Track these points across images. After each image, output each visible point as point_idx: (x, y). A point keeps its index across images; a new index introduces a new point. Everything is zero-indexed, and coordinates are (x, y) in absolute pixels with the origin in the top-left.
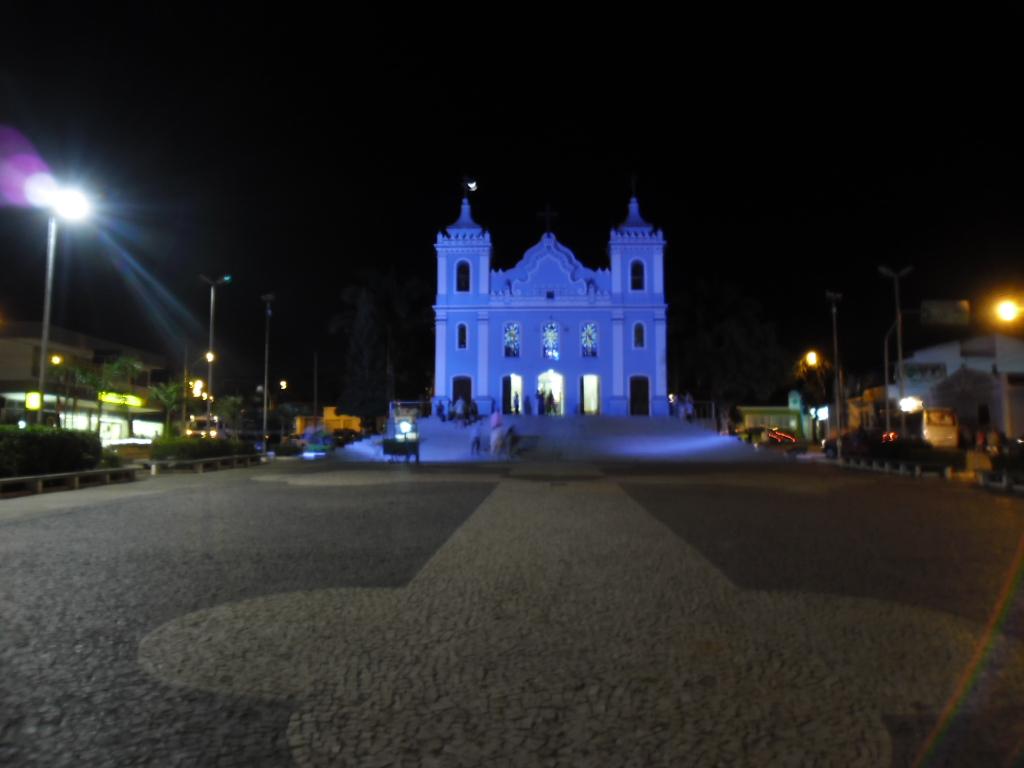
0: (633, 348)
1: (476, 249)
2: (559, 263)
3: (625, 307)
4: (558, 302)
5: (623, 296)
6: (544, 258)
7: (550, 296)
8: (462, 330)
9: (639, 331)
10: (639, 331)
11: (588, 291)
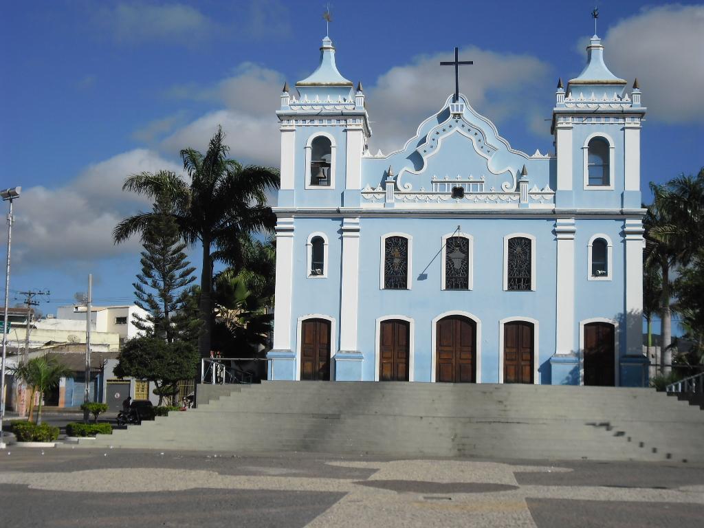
0: (590, 278)
6: (453, 131)
7: (458, 193)
9: (600, 248)
10: (600, 248)
11: (518, 187)
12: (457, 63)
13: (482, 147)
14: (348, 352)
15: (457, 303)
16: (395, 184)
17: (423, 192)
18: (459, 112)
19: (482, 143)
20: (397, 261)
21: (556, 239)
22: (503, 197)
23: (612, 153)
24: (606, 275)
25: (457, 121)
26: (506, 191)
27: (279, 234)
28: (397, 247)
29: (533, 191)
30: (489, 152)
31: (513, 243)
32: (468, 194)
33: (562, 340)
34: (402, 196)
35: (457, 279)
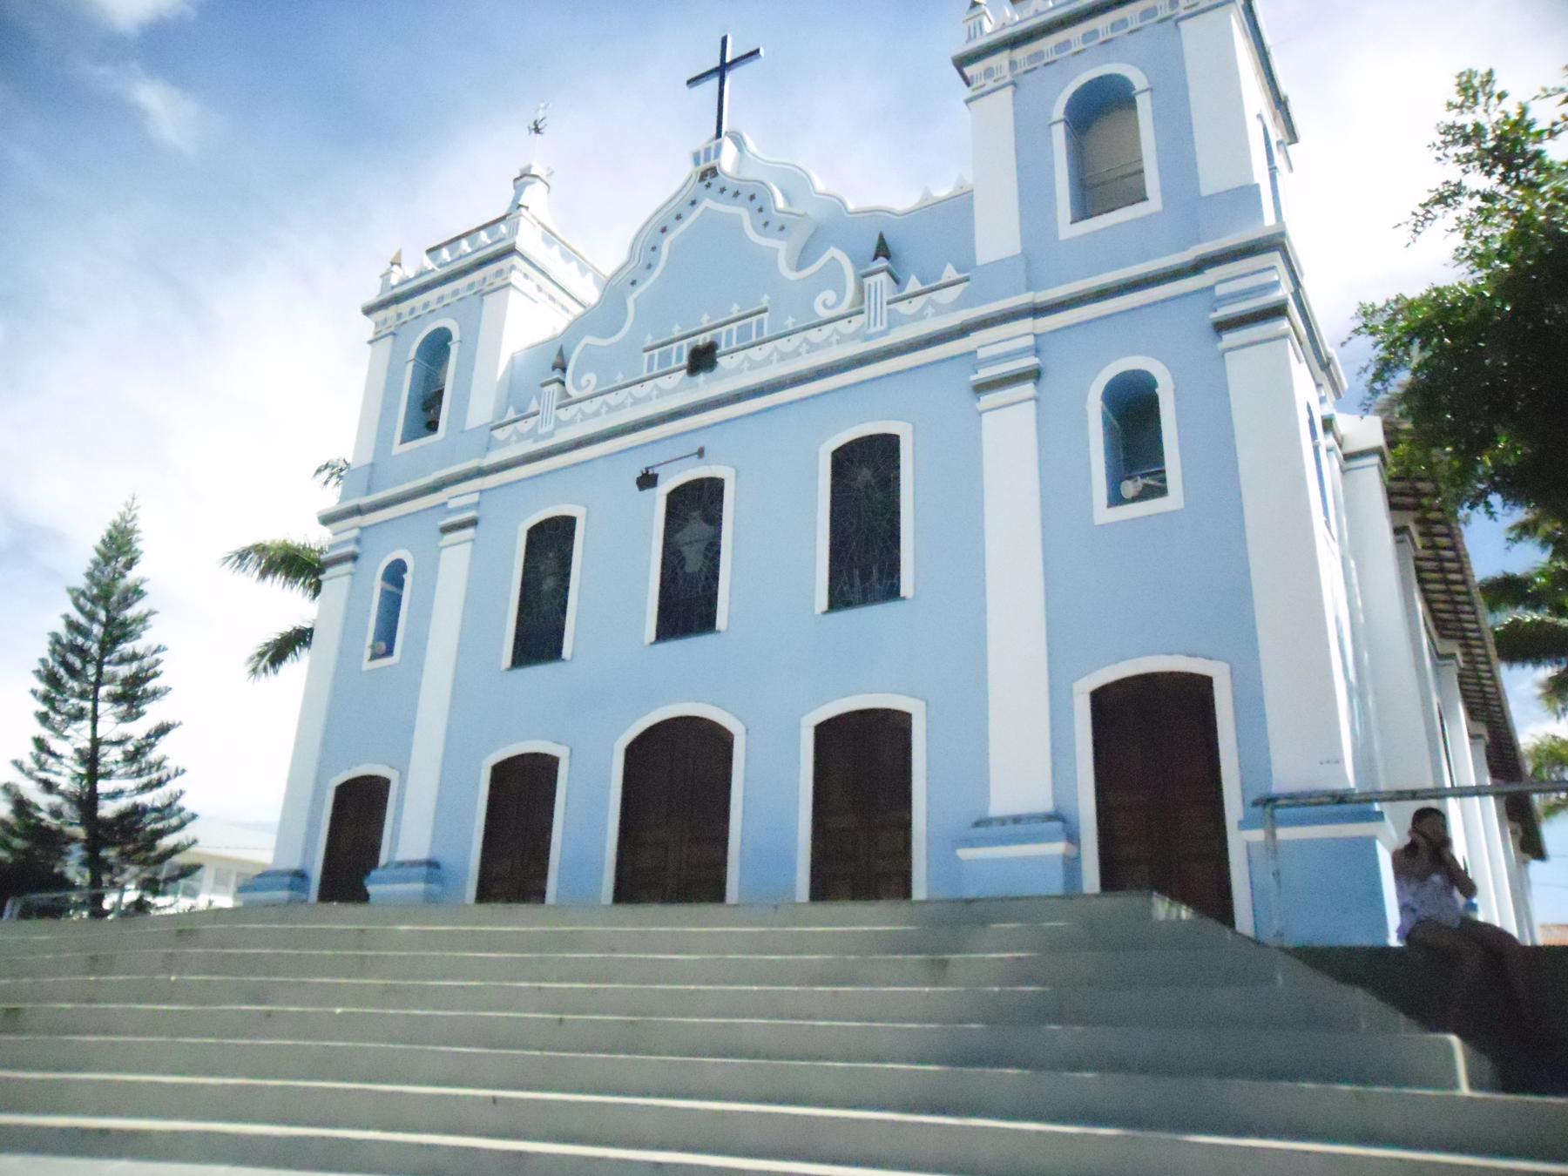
0: (1103, 514)
1: (476, 276)
2: (743, 212)
3: (1037, 311)
4: (731, 373)
5: (1029, 264)
6: (699, 210)
7: (702, 359)
8: (395, 574)
12: (722, 70)
13: (766, 224)
14: (401, 864)
15: (685, 684)
16: (563, 383)
17: (620, 383)
18: (712, 162)
19: (762, 218)
20: (549, 584)
21: (980, 414)
22: (814, 335)
23: (1144, 104)
24: (1161, 491)
25: (708, 186)
26: (825, 314)
27: (330, 572)
28: (551, 544)
29: (909, 289)
30: (782, 228)
31: (845, 459)
32: (724, 354)
33: (1011, 766)
34: (573, 409)
35: (687, 606)
